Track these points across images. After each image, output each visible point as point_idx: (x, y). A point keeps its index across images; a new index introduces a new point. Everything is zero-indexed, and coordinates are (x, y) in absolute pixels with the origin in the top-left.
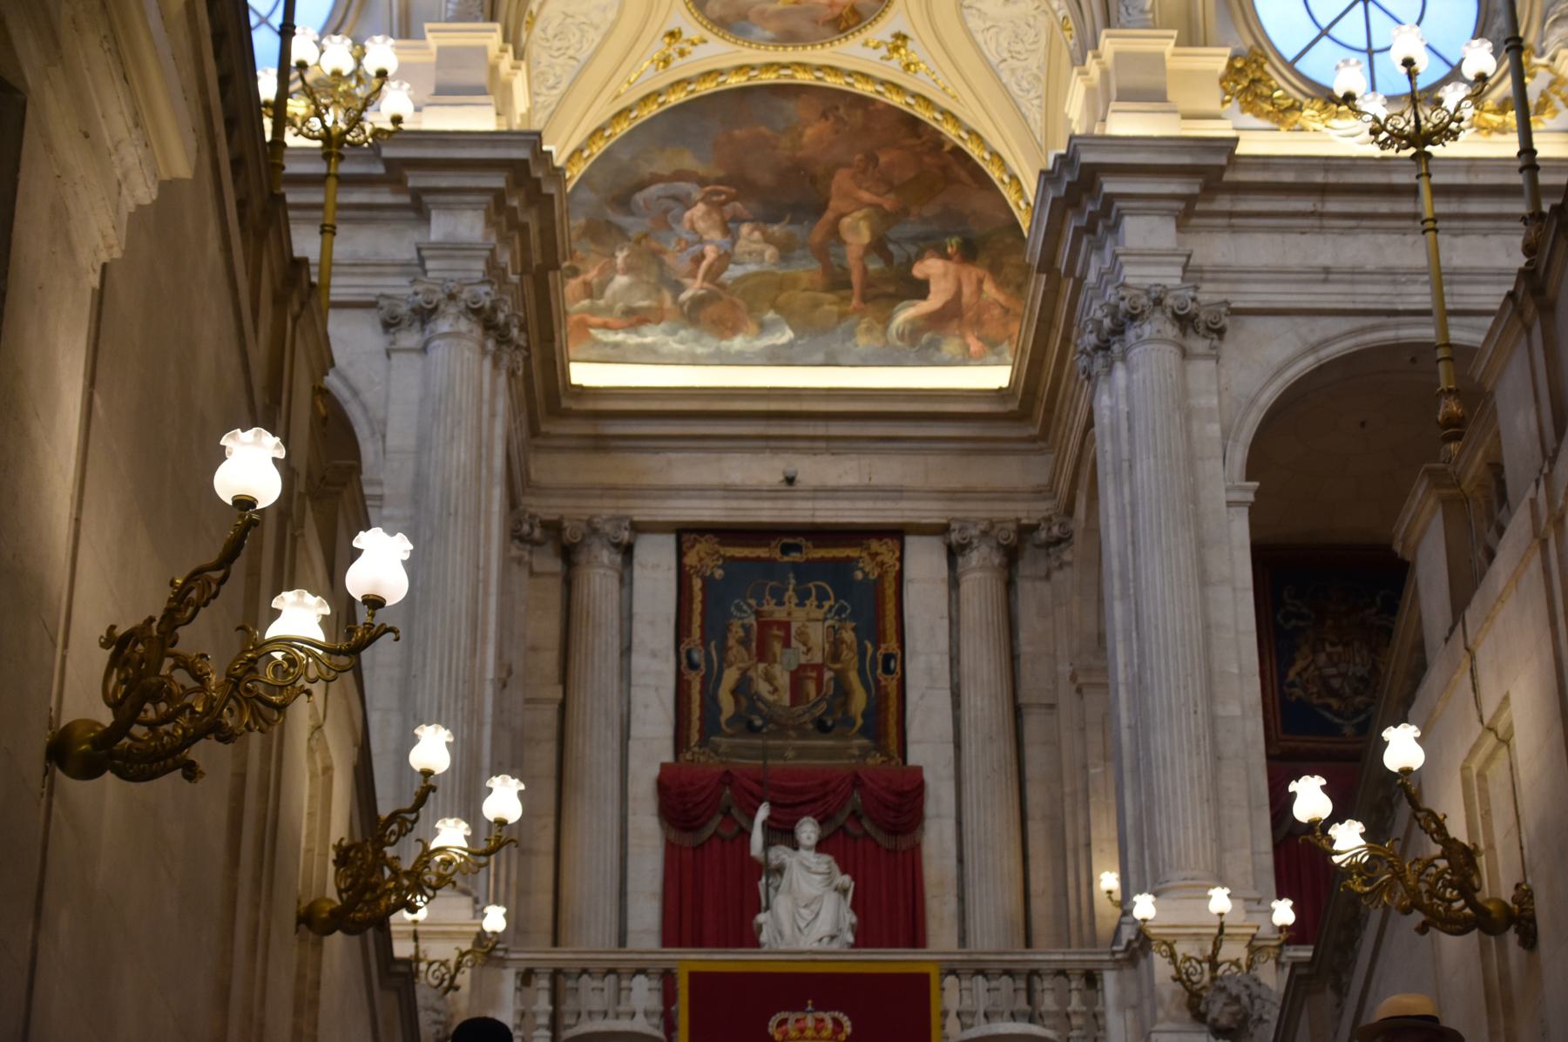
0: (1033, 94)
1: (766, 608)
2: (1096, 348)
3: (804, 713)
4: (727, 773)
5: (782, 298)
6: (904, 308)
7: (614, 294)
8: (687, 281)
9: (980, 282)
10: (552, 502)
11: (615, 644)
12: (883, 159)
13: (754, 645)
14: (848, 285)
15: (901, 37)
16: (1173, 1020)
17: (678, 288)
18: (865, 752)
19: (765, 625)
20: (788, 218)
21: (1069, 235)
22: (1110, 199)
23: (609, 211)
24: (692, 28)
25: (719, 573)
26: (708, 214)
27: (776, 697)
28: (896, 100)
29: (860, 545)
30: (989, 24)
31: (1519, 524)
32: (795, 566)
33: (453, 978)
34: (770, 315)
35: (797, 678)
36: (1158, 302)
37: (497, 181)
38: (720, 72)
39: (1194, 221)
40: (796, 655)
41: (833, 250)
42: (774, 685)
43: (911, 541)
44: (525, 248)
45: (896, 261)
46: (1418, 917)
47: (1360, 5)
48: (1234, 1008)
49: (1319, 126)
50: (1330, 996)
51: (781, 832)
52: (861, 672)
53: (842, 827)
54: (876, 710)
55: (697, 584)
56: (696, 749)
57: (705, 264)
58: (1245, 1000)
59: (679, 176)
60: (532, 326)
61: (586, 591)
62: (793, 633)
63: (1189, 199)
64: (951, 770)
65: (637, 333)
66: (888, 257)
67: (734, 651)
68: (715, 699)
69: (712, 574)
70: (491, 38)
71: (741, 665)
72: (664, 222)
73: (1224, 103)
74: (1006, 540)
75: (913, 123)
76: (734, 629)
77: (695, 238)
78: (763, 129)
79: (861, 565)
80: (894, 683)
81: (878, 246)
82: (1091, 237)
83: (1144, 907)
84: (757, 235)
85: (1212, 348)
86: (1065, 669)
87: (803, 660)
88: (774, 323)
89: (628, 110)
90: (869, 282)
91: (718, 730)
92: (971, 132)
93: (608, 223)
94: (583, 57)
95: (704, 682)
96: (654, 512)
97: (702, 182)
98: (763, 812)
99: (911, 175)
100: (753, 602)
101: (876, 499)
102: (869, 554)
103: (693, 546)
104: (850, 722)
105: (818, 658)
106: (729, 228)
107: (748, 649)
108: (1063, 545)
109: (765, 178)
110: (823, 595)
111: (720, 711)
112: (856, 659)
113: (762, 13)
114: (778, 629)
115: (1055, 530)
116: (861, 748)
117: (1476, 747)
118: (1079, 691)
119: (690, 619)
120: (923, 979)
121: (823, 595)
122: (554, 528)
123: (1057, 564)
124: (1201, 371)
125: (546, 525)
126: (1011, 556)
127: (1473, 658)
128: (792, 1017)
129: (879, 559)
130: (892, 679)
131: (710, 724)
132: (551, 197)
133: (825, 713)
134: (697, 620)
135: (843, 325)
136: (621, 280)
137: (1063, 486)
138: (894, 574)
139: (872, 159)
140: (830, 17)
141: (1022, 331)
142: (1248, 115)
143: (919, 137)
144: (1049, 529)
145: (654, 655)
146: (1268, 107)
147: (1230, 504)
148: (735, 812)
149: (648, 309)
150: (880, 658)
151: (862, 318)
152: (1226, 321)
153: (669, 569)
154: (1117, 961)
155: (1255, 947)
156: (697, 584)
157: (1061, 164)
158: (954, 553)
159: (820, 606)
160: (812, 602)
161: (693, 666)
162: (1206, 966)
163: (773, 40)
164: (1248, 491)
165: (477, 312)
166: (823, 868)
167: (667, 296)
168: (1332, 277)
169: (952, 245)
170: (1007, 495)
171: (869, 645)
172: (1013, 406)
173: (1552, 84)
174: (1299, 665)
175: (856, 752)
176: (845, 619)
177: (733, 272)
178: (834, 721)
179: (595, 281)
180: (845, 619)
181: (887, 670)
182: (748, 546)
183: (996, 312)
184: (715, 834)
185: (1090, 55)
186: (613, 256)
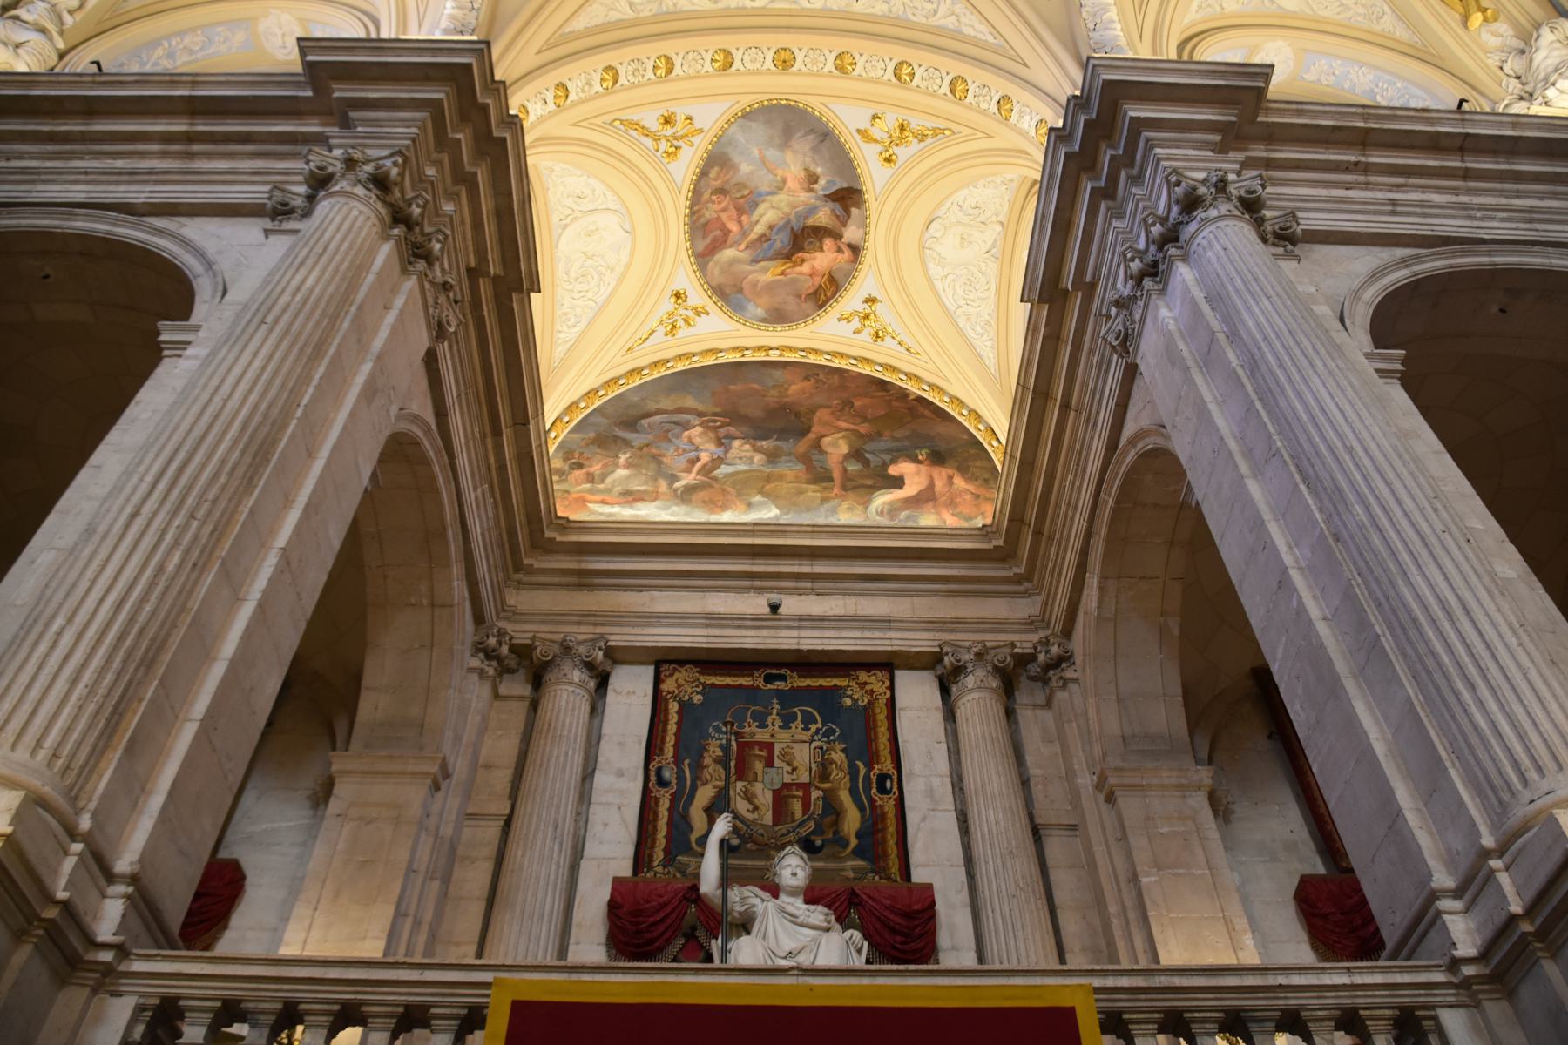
0: (985, 337)
1: (747, 729)
3: (789, 832)
5: (768, 487)
6: (882, 494)
7: (614, 481)
8: (683, 475)
9: (950, 478)
11: (577, 760)
12: (857, 404)
13: (733, 764)
14: (831, 479)
15: (871, 300)
17: (673, 478)
20: (775, 437)
22: (1139, 124)
23: (617, 429)
25: (697, 698)
27: (756, 815)
28: (866, 370)
29: (849, 675)
30: (947, 271)
32: (779, 694)
34: (758, 498)
35: (780, 799)
40: (781, 774)
41: (814, 457)
43: (902, 677)
45: (872, 465)
52: (853, 791)
55: (674, 707)
56: (659, 869)
57: (699, 465)
59: (680, 410)
61: (550, 706)
62: (776, 753)
65: (632, 507)
66: (866, 463)
67: (710, 769)
68: (685, 817)
69: (691, 698)
71: (718, 783)
72: (666, 437)
74: (1001, 662)
75: (882, 384)
76: (711, 749)
77: (692, 448)
79: (849, 693)
80: (892, 802)
81: (856, 454)
82: (1110, 203)
87: (787, 779)
88: (760, 504)
94: (600, 299)
96: (633, 638)
99: (883, 413)
101: (863, 629)
102: (857, 683)
103: (672, 675)
104: (842, 842)
105: (805, 778)
108: (1064, 665)
109: (756, 413)
110: (808, 720)
111: (691, 829)
112: (848, 777)
113: (755, 284)
114: (761, 750)
115: (1055, 649)
116: (854, 870)
119: (663, 740)
121: (808, 720)
122: (523, 652)
123: (1061, 683)
129: (868, 687)
130: (890, 798)
133: (813, 833)
134: (670, 740)
135: (825, 506)
136: (621, 473)
138: (885, 701)
139: (848, 403)
140: (811, 291)
143: (887, 391)
144: (1048, 652)
145: (620, 774)
149: (645, 492)
150: (874, 778)
151: (843, 501)
153: (645, 696)
154: (1466, 983)
156: (674, 707)
157: (1075, 105)
159: (808, 729)
161: (662, 783)
163: (764, 320)
167: (663, 485)
168: (1399, 209)
169: (922, 454)
170: (998, 625)
171: (861, 766)
175: (851, 875)
176: (834, 741)
178: (823, 840)
179: (598, 472)
180: (834, 741)
181: (882, 789)
182: (730, 675)
183: (968, 497)
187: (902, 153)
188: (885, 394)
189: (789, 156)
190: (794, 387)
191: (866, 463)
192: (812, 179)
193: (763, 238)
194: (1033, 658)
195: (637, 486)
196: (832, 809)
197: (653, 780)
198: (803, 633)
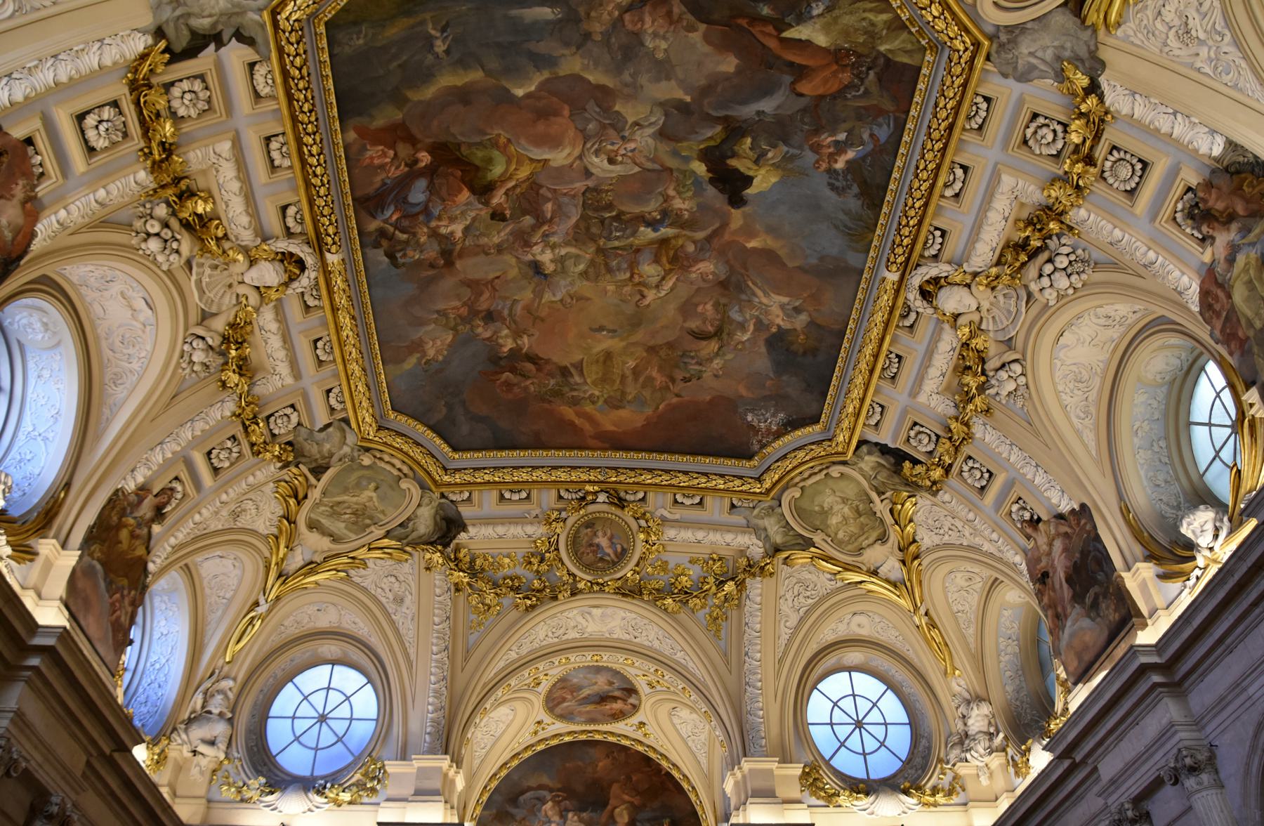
12: (634, 778)
15: (642, 724)
24: (547, 719)
26: (553, 807)
38: (561, 735)
47: (858, 730)
49: (849, 805)
70: (444, 762)
73: (802, 791)
84: (576, 818)
89: (518, 754)
92: (674, 765)
94: (497, 735)
97: (551, 790)
99: (646, 786)
113: (580, 712)
139: (629, 778)
146: (823, 794)
173: (954, 778)
187: (659, 688)
188: (648, 769)
189: (599, 676)
192: (611, 683)
193: (583, 698)
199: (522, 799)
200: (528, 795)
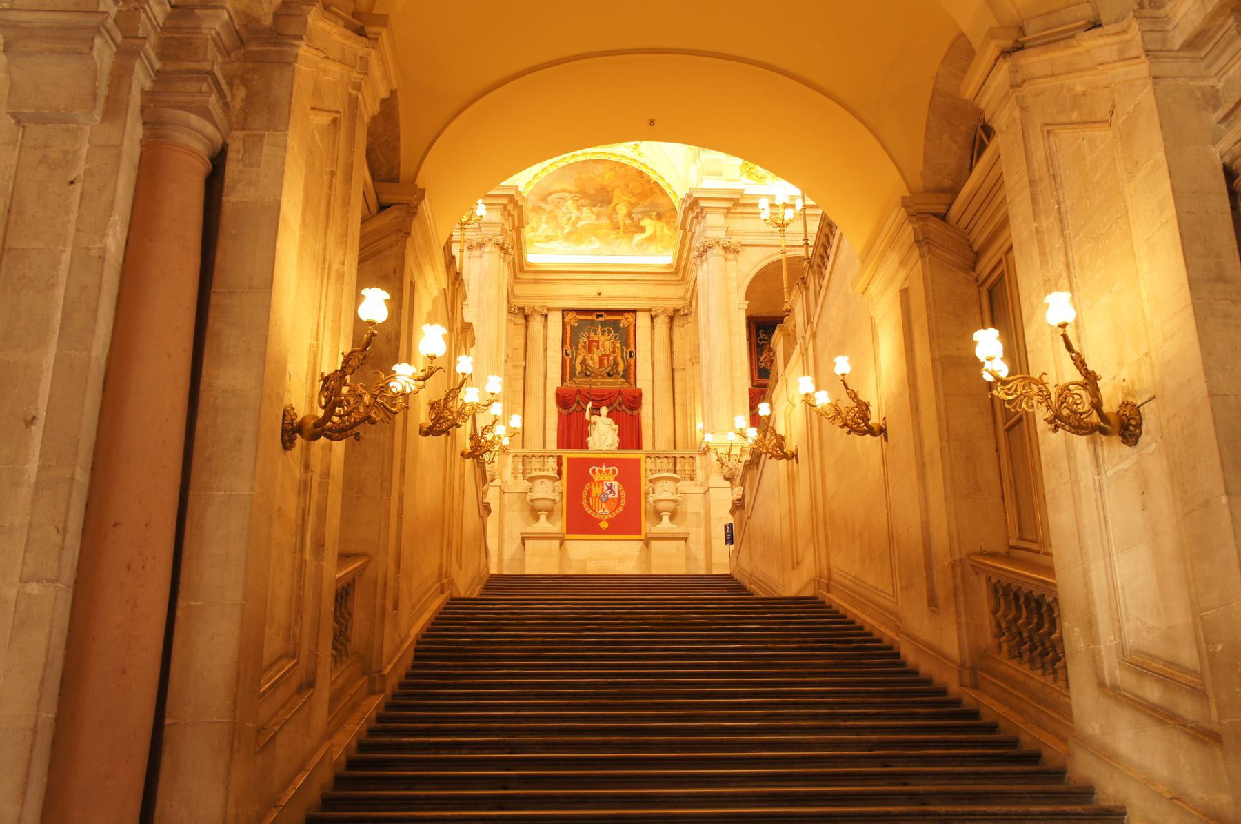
2: (698, 256)
4: (578, 390)
5: (597, 232)
8: (565, 226)
9: (663, 227)
10: (522, 300)
12: (631, 186)
14: (619, 228)
16: (717, 473)
17: (563, 229)
18: (623, 383)
19: (590, 342)
21: (690, 218)
22: (702, 209)
25: (576, 324)
31: (797, 348)
32: (601, 321)
33: (493, 459)
34: (593, 238)
36: (718, 243)
37: (505, 201)
39: (730, 215)
40: (601, 352)
41: (613, 216)
42: (593, 362)
43: (638, 313)
44: (513, 222)
46: (769, 455)
48: (730, 472)
50: (755, 469)
51: (596, 411)
52: (622, 357)
53: (616, 408)
54: (626, 370)
55: (569, 328)
57: (571, 221)
58: (734, 469)
59: (563, 191)
60: (516, 248)
63: (729, 209)
64: (651, 389)
66: (632, 219)
68: (574, 366)
72: (558, 207)
75: (641, 173)
78: (591, 175)
81: (629, 215)
83: (709, 438)
84: (589, 211)
85: (735, 257)
86: (688, 357)
87: (603, 353)
90: (626, 228)
91: (575, 376)
93: (539, 207)
95: (571, 360)
98: (590, 405)
99: (640, 190)
100: (587, 334)
105: (608, 353)
106: (579, 210)
107: (585, 349)
109: (591, 191)
110: (610, 332)
115: (686, 311)
117: (787, 408)
118: (692, 364)
119: (566, 340)
120: (639, 461)
121: (610, 332)
122: (522, 309)
124: (731, 264)
125: (519, 308)
126: (671, 319)
127: (787, 382)
128: (597, 469)
129: (628, 320)
131: (573, 374)
132: (521, 206)
136: (544, 226)
137: (688, 297)
141: (676, 245)
142: (749, 180)
145: (555, 351)
146: (755, 177)
147: (739, 308)
148: (581, 402)
152: (739, 249)
155: (742, 450)
156: (569, 328)
158: (652, 318)
159: (609, 335)
160: (606, 334)
161: (567, 355)
162: (727, 456)
164: (745, 304)
165: (498, 244)
166: (609, 423)
167: (559, 231)
169: (654, 214)
170: (670, 299)
172: (673, 270)
174: (764, 356)
177: (581, 224)
181: (630, 356)
183: (668, 237)
184: (575, 410)
185: (698, 159)
186: (541, 218)
190: (606, 176)
191: (632, 219)
194: (679, 310)
195: (550, 233)
196: (616, 363)
197: (565, 354)
198: (609, 302)
199: (549, 198)
200: (554, 196)
